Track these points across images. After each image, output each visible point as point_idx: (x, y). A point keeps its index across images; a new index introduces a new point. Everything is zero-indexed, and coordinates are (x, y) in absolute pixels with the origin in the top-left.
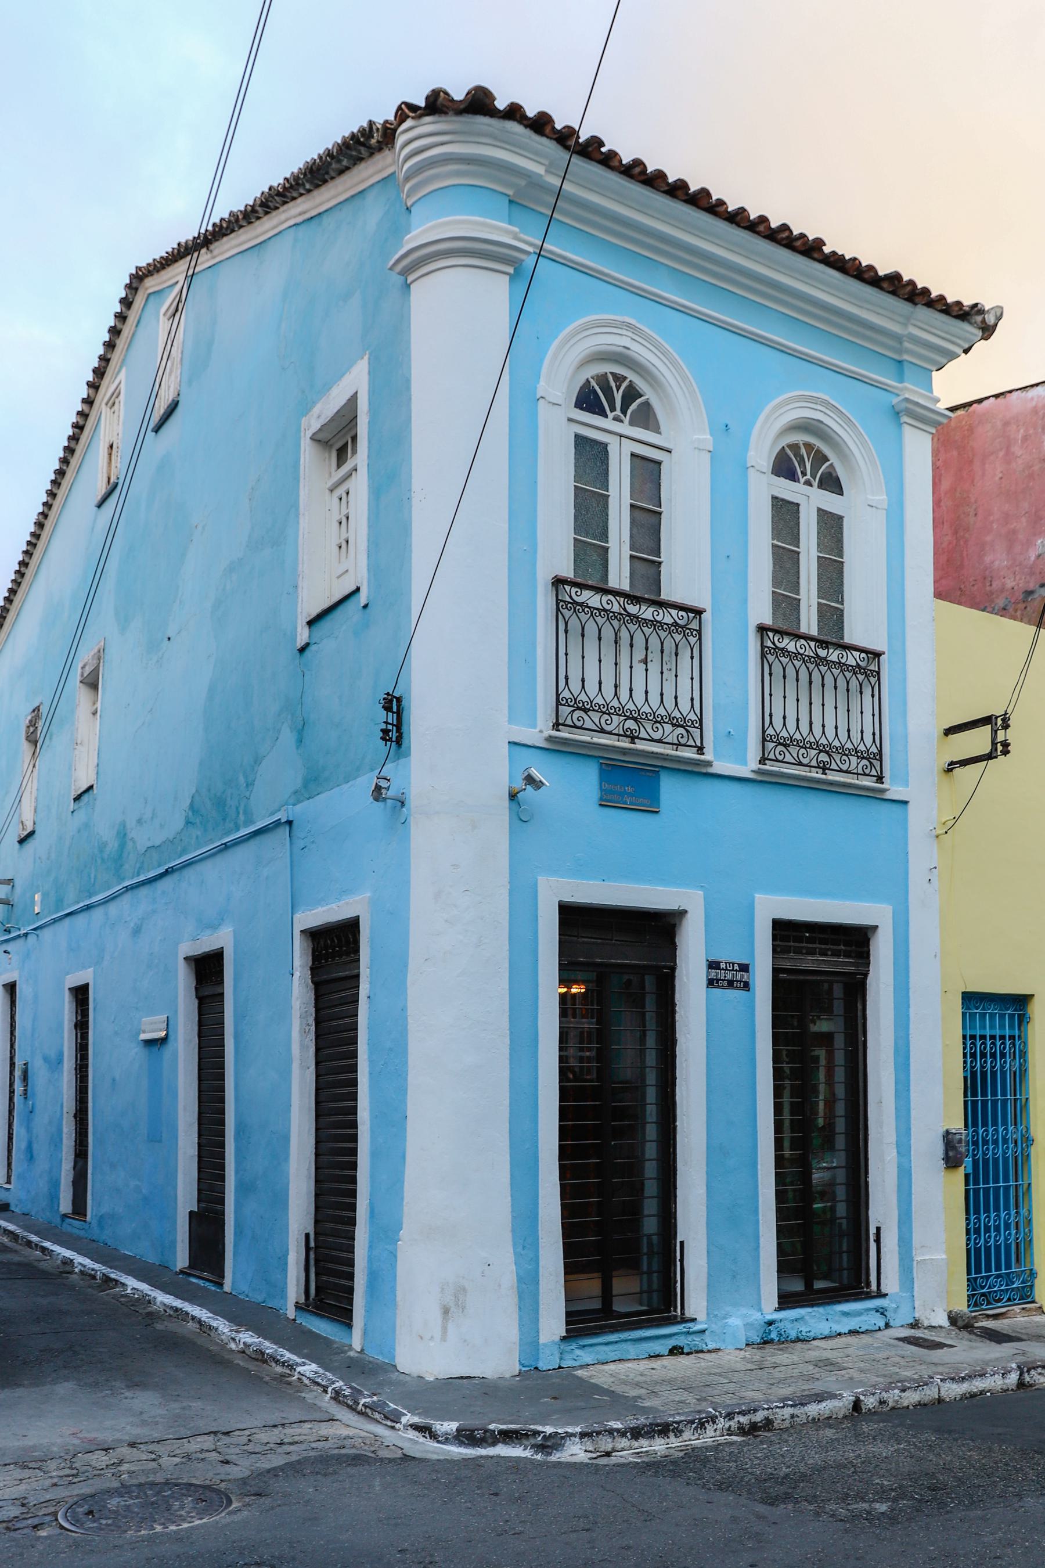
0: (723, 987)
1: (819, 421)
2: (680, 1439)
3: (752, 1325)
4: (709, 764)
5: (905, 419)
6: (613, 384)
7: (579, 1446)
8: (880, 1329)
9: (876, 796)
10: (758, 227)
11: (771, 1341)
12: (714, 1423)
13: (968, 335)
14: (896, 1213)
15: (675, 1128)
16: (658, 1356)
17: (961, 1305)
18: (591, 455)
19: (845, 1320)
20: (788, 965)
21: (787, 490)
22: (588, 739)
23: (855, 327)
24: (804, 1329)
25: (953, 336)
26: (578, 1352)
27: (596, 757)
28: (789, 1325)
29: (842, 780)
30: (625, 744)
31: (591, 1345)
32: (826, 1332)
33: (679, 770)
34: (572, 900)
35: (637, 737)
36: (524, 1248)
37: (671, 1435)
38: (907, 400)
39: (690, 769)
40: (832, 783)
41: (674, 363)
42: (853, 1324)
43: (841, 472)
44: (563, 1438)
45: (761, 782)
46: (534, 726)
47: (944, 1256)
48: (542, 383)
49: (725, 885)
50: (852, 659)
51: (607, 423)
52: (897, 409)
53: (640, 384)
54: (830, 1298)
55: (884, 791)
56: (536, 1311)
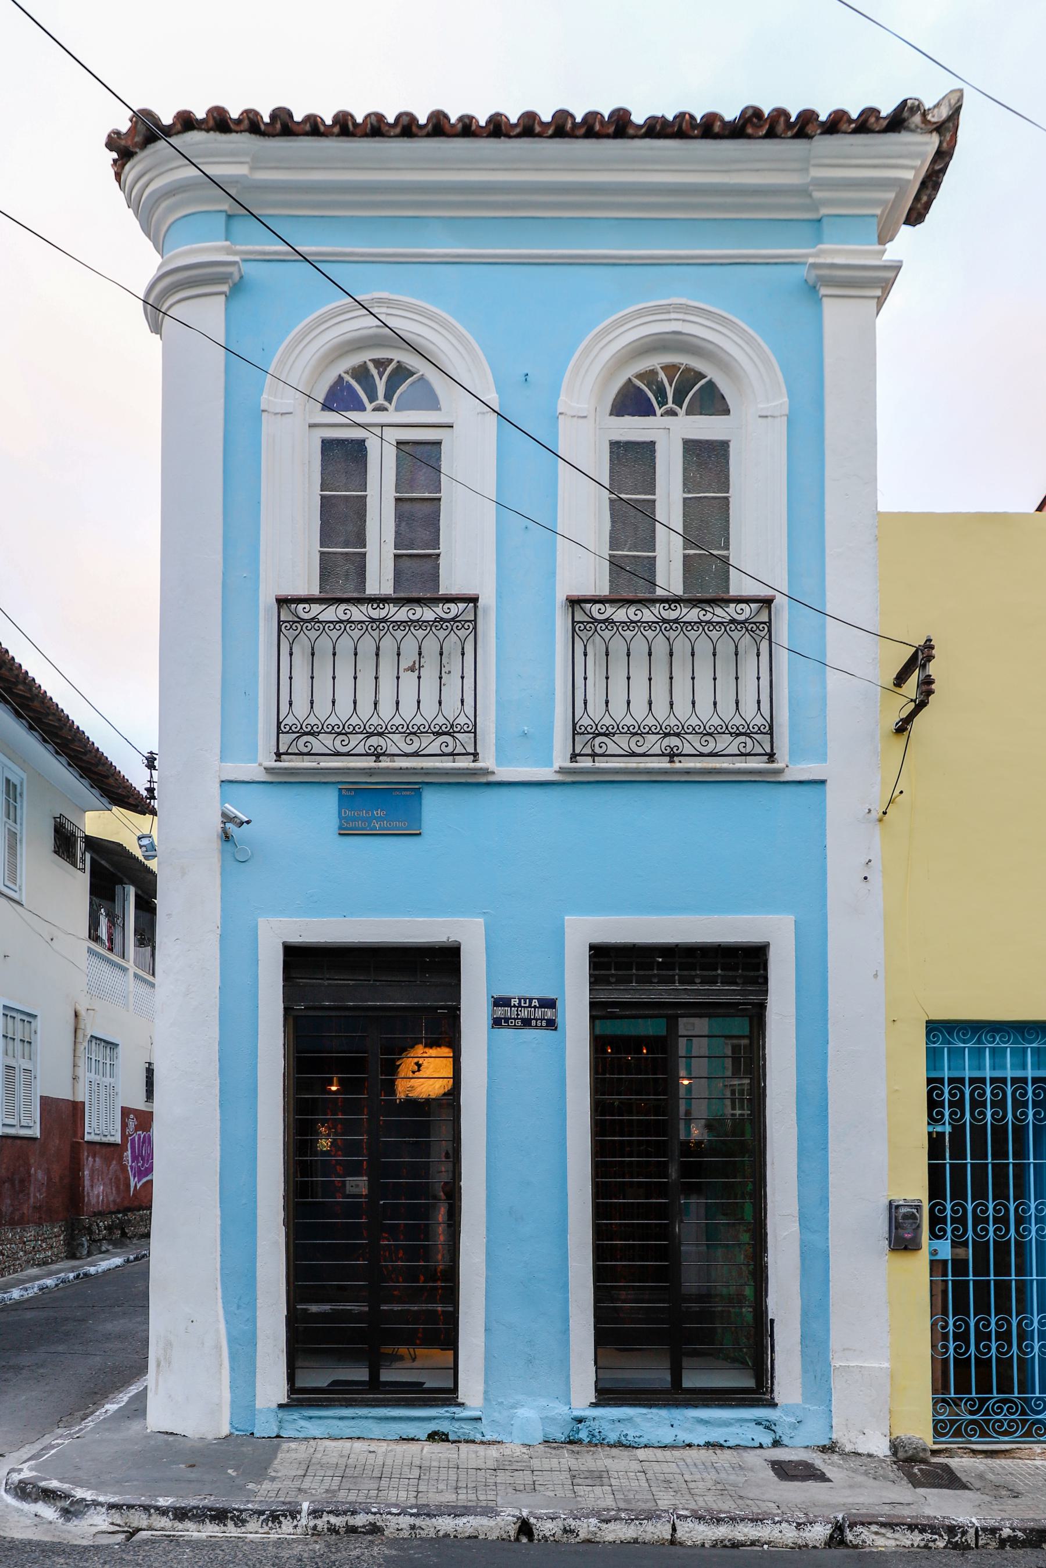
0: (515, 1027)
1: (674, 333)
2: (243, 1529)
3: (553, 1419)
4: (486, 772)
5: (823, 291)
6: (374, 372)
7: (104, 1517)
8: (761, 1446)
9: (770, 779)
10: (563, 127)
11: (579, 1442)
12: (294, 1518)
13: (913, 148)
14: (797, 1303)
15: (460, 1188)
16: (413, 1439)
17: (919, 1430)
18: (344, 458)
19: (702, 1429)
20: (603, 997)
21: (633, 428)
22: (314, 765)
23: (729, 200)
24: (631, 1433)
25: (888, 157)
26: (303, 1423)
27: (333, 783)
28: (606, 1427)
29: (699, 765)
30: (369, 763)
31: (320, 1418)
32: (668, 1440)
33: (449, 784)
34: (300, 940)
35: (384, 754)
36: (239, 1307)
37: (230, 1524)
38: (814, 266)
39: (463, 780)
40: (688, 772)
41: (444, 324)
42: (715, 1435)
43: (724, 386)
44: (87, 1506)
45: (574, 783)
46: (255, 760)
47: (886, 1365)
48: (265, 396)
49: (524, 907)
50: (746, 611)
51: (367, 417)
52: (811, 282)
53: (411, 360)
54: (619, 1399)
55: (780, 771)
56: (254, 1373)
